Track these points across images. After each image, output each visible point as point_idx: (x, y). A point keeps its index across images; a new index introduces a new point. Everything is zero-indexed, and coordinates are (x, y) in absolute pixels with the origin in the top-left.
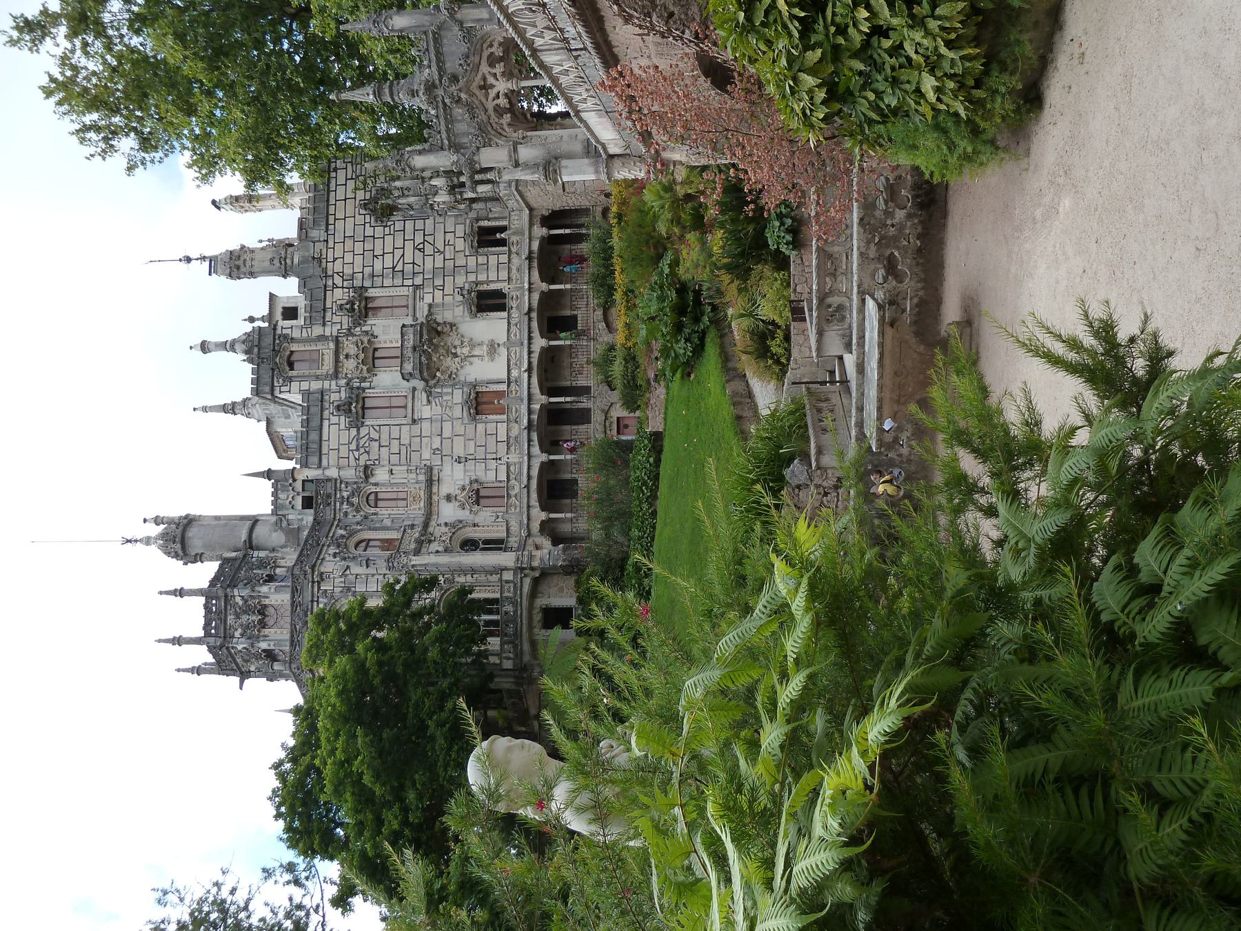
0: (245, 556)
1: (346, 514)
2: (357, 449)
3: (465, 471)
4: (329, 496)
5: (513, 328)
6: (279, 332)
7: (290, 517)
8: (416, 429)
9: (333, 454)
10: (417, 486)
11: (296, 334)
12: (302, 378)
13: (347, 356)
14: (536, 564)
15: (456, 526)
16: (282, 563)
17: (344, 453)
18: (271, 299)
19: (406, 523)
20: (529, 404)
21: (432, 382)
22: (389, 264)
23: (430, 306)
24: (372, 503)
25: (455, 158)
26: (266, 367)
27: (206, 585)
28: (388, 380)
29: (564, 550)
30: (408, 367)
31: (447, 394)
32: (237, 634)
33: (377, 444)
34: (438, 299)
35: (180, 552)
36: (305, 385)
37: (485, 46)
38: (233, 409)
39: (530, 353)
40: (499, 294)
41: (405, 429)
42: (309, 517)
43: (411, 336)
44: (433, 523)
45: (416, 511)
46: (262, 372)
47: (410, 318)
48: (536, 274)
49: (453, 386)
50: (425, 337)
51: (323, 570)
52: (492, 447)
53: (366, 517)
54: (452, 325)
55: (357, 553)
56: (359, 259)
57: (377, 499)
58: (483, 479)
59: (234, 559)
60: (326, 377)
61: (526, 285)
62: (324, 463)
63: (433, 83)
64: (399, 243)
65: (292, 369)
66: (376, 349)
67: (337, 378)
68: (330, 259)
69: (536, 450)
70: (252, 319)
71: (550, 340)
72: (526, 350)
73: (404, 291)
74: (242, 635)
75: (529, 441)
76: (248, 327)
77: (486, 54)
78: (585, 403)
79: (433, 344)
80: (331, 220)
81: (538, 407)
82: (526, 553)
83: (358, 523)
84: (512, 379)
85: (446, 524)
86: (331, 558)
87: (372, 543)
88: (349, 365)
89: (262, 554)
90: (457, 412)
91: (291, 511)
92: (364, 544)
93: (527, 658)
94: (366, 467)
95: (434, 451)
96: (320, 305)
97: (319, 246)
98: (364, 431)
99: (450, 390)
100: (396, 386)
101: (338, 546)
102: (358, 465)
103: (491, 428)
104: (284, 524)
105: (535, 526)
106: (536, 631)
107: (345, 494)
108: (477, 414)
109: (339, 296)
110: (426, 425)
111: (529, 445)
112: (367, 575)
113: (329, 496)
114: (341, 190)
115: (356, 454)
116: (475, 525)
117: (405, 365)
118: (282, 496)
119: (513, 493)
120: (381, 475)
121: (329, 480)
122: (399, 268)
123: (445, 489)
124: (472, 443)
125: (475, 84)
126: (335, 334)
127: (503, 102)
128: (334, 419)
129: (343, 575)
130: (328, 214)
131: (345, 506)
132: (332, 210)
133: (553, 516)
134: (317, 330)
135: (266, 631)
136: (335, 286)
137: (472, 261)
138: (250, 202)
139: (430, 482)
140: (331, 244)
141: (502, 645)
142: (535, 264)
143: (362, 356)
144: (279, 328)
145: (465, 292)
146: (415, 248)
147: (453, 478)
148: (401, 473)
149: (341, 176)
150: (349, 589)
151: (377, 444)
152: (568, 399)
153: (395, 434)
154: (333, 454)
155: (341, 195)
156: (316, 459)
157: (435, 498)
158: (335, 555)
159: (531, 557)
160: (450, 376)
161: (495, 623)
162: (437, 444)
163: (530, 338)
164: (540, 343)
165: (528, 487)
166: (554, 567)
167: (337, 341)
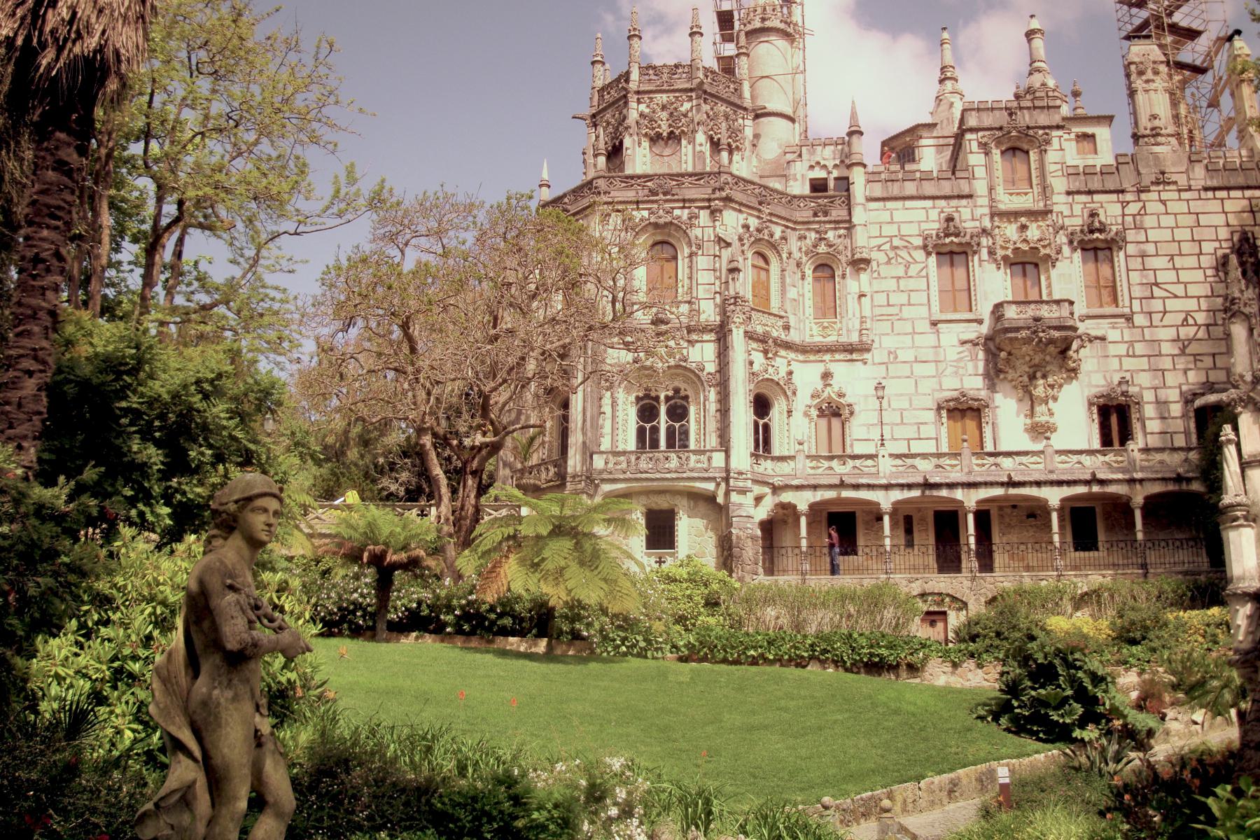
0: (745, 109)
2: (895, 248)
3: (866, 397)
4: (826, 214)
5: (1075, 458)
6: (1055, 133)
8: (924, 326)
9: (885, 216)
12: (989, 168)
14: (734, 497)
15: (785, 387)
16: (736, 157)
17: (890, 230)
23: (1103, 339)
26: (1001, 119)
28: (994, 284)
29: (753, 538)
30: (1011, 313)
31: (976, 367)
32: (642, 107)
33: (902, 274)
34: (1113, 350)
35: (749, 27)
36: (980, 172)
39: (1038, 484)
40: (1126, 435)
41: (923, 311)
42: (800, 187)
43: (1057, 315)
44: (792, 355)
45: (806, 329)
46: (997, 113)
47: (1084, 311)
48: (1157, 488)
50: (1056, 334)
52: (901, 432)
54: (1074, 371)
59: (741, 97)
60: (992, 200)
61: (1138, 475)
64: (1193, 290)
65: (1003, 153)
66: (1036, 265)
68: (1164, 196)
69: (897, 495)
71: (1061, 510)
72: (1042, 478)
74: (642, 115)
75: (910, 486)
78: (970, 562)
79: (1047, 345)
80: (1223, 194)
81: (959, 494)
82: (749, 484)
84: (1000, 460)
85: (790, 373)
86: (742, 222)
87: (763, 274)
88: (1011, 231)
91: (807, 165)
93: (606, 487)
94: (867, 261)
96: (1095, 184)
98: (920, 255)
101: (759, 230)
102: (871, 249)
103: (929, 431)
104: (790, 157)
105: (787, 497)
106: (643, 500)
107: (830, 235)
108: (948, 411)
109: (1111, 210)
110: (931, 339)
111: (902, 486)
113: (826, 214)
115: (887, 247)
116: (790, 412)
117: (1014, 307)
118: (829, 151)
119: (835, 463)
121: (850, 214)
124: (907, 405)
126: (1056, 208)
128: (934, 214)
129: (720, 240)
130: (1228, 189)
132: (1233, 194)
133: (803, 521)
134: (1059, 184)
135: (646, 144)
136: (1125, 204)
137: (1174, 395)
139: (850, 349)
140: (1185, 195)
141: (624, 453)
142: (1171, 487)
143: (1025, 247)
145: (1124, 388)
146: (1188, 313)
147: (852, 381)
150: (699, 247)
151: (902, 274)
152: (972, 540)
153: (915, 298)
154: (885, 216)
156: (878, 194)
157: (827, 357)
158: (746, 227)
159: (743, 492)
160: (1001, 371)
161: (655, 444)
162: (902, 356)
163: (1060, 483)
164: (1054, 496)
165: (842, 485)
166: (730, 525)
167: (1045, 213)
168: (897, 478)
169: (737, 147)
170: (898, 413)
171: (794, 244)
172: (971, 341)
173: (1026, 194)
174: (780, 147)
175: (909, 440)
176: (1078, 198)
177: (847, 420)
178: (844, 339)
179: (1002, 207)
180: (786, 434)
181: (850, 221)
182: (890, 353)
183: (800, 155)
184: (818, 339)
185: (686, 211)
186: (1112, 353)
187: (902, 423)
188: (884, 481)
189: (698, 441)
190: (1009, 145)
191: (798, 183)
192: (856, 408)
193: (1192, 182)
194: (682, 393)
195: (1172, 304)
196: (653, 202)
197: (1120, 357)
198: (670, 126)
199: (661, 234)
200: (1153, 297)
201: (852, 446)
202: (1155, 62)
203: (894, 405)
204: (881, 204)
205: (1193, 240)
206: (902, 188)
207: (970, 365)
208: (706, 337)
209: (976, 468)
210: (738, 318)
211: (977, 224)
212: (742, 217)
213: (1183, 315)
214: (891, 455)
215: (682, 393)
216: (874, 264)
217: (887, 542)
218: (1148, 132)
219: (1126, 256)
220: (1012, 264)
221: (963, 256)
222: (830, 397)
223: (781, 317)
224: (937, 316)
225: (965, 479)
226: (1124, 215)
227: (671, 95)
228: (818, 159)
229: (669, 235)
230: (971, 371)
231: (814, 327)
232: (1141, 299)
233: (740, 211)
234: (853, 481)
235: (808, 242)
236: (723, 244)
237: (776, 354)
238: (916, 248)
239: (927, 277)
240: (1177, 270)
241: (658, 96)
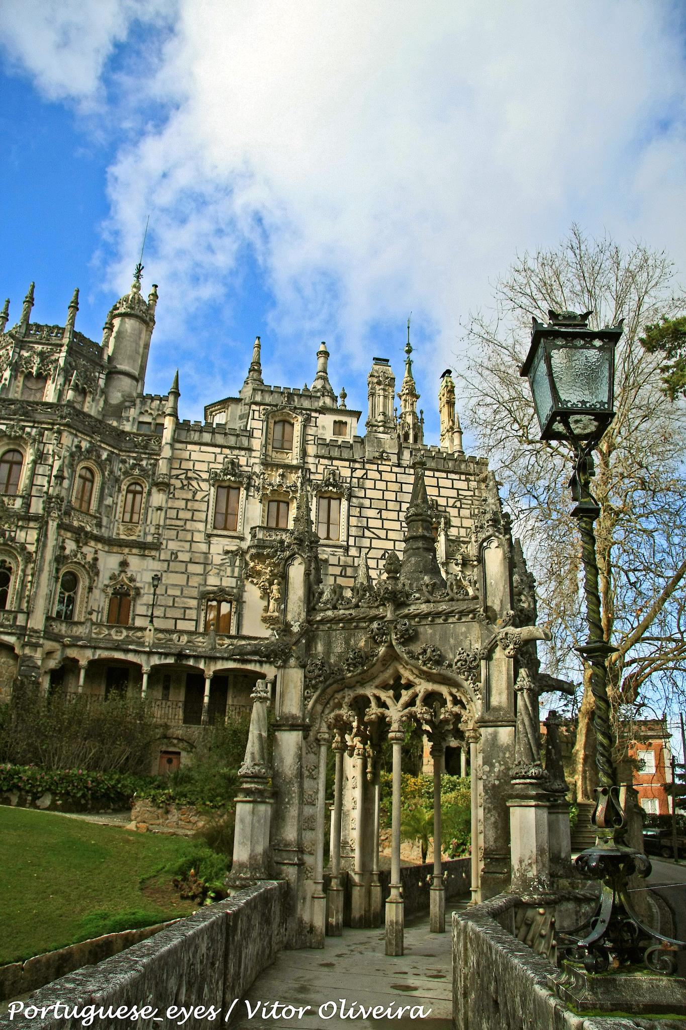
0: (102, 366)
1: (124, 462)
2: (187, 478)
6: (313, 414)
7: (132, 410)
8: (199, 537)
9: (186, 455)
10: (142, 534)
11: (311, 431)
13: (283, 476)
16: (89, 399)
18: (355, 412)
19: (105, 521)
20: (205, 658)
21: (248, 557)
22: (372, 523)
24: (132, 488)
25: (296, 629)
27: (77, 329)
31: (233, 571)
33: (190, 496)
37: (454, 691)
38: (254, 370)
41: (201, 526)
44: (100, 546)
49: (239, 578)
51: (65, 434)
53: (117, 480)
55: (79, 468)
56: (379, 495)
57: (135, 493)
58: (139, 602)
62: (178, 446)
63: (405, 605)
64: (392, 535)
65: (275, 423)
67: (262, 464)
68: (381, 468)
69: (155, 660)
70: (344, 396)
73: (343, 537)
76: (337, 392)
77: (444, 690)
81: (202, 666)
82: (41, 641)
83: (111, 472)
85: (96, 559)
86: (76, 443)
87: (88, 484)
89: (102, 382)
90: (213, 581)
91: (138, 411)
92: (88, 475)
94: (168, 485)
95: (175, 554)
96: (335, 453)
97: (394, 459)
98: (205, 486)
99: (236, 574)
100: (245, 520)
101: (89, 451)
103: (192, 614)
104: (127, 404)
105: (72, 653)
107: (144, 463)
110: (203, 547)
111: (161, 654)
112: (50, 476)
114: (448, 483)
115: (183, 477)
119: (113, 632)
120: (158, 498)
121: (160, 449)
122: (367, 533)
123: (135, 562)
124: (178, 593)
125: (402, 671)
127: (373, 711)
128: (220, 458)
131: (132, 461)
134: (311, 450)
136: (353, 470)
138: (448, 402)
140: (395, 469)
144: (316, 415)
146: (386, 550)
147: (142, 569)
148: (156, 518)
149: (462, 485)
151: (190, 496)
152: (206, 700)
155: (443, 482)
157: (126, 550)
158: (79, 447)
159: (35, 646)
162: (183, 557)
165: (117, 649)
168: (157, 648)
169: (90, 392)
170: (171, 599)
171: (117, 467)
172: (232, 552)
173: (287, 453)
174: (123, 396)
175: (176, 619)
176: (322, 461)
177: (134, 599)
178: (142, 540)
179: (269, 459)
180: (85, 605)
181: (159, 455)
182: (172, 553)
183: (135, 405)
184: (123, 537)
185: (34, 430)
186: (330, 573)
187: (173, 606)
188: (148, 649)
189: (12, 604)
190: (281, 418)
191: (130, 423)
192: (142, 591)
193: (402, 462)
194: (7, 565)
195: (376, 543)
196: (11, 420)
197: (335, 576)
198: (40, 368)
199: (14, 444)
200: (363, 537)
201: (133, 619)
202: (387, 378)
203: (170, 592)
204: (184, 445)
205: (396, 501)
206: (201, 437)
207: (229, 569)
208: (32, 524)
209: (218, 647)
210: (55, 514)
211: (250, 469)
212: (76, 440)
213: (383, 552)
214: (156, 629)
215: (7, 565)
216: (172, 488)
217: (143, 695)
218: (376, 423)
219: (349, 506)
220: (270, 501)
221: (236, 491)
222: (123, 581)
223: (96, 517)
224: (209, 532)
225: (209, 654)
226: (352, 477)
227: (45, 347)
228: (147, 409)
229: (20, 446)
230: (229, 574)
231: (121, 528)
232: (355, 537)
233: (76, 436)
234: (125, 647)
235: (127, 465)
236: (56, 458)
237: (86, 544)
238: (204, 480)
239: (208, 502)
240: (383, 520)
241: (36, 346)
